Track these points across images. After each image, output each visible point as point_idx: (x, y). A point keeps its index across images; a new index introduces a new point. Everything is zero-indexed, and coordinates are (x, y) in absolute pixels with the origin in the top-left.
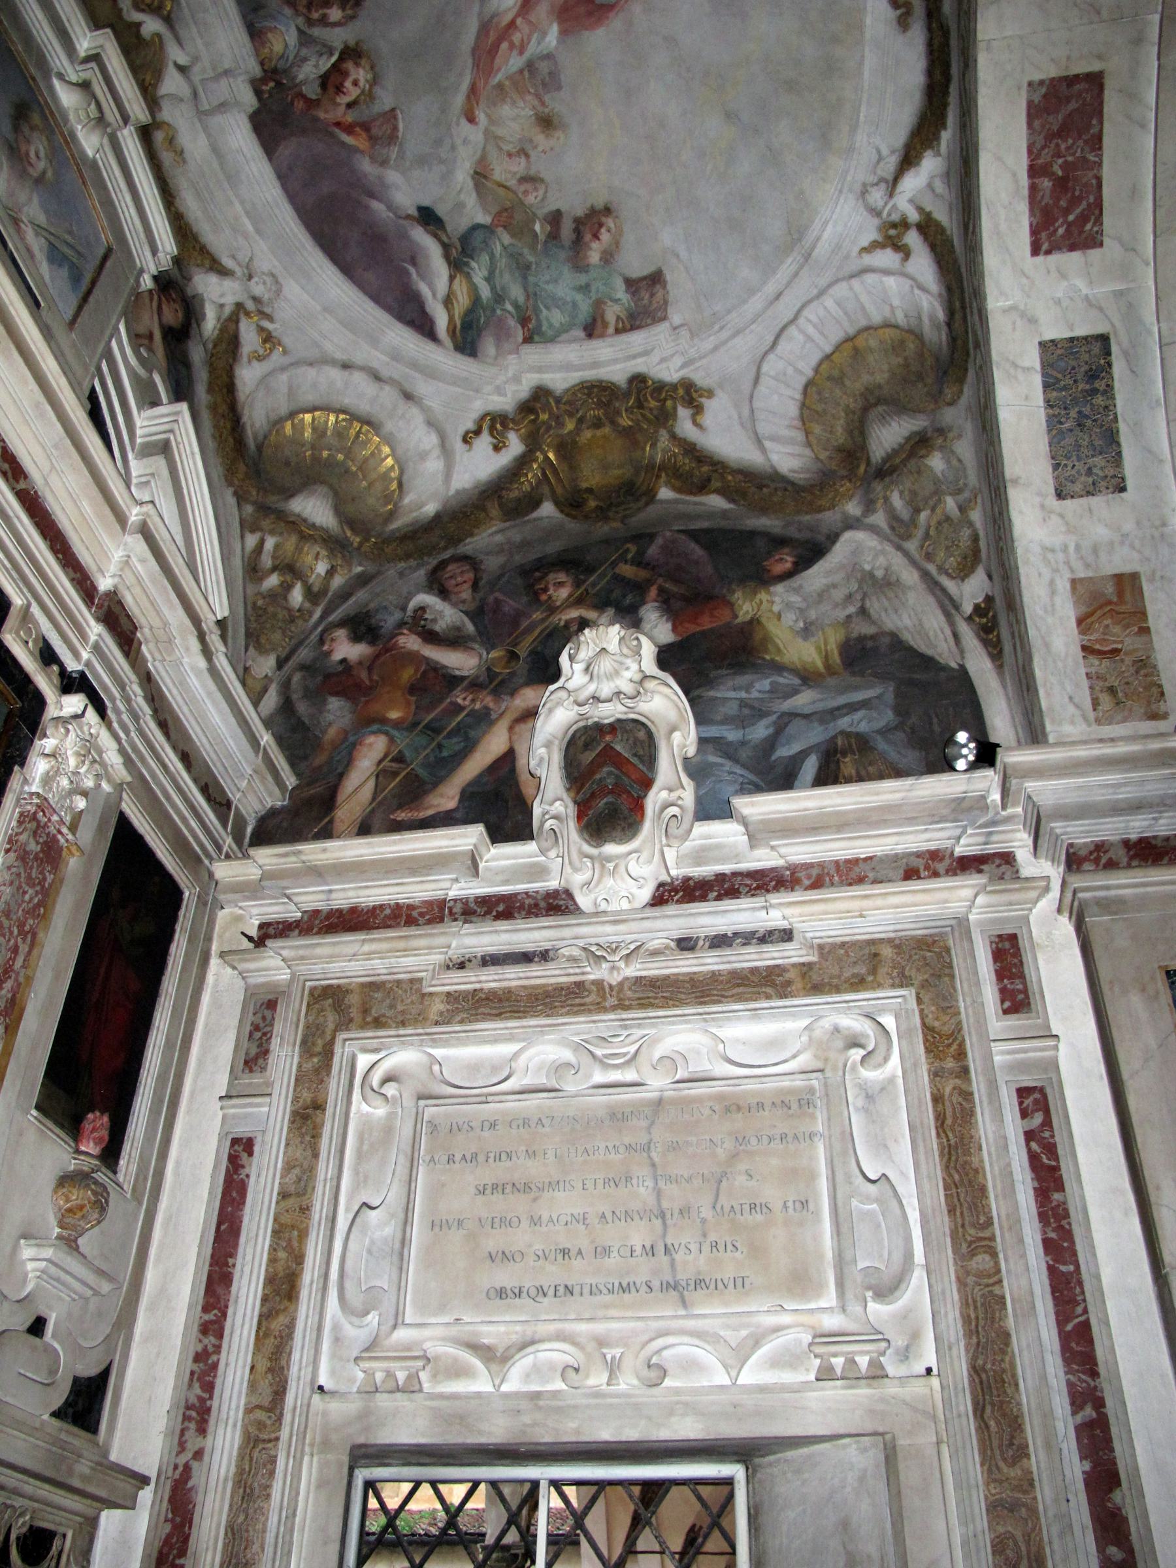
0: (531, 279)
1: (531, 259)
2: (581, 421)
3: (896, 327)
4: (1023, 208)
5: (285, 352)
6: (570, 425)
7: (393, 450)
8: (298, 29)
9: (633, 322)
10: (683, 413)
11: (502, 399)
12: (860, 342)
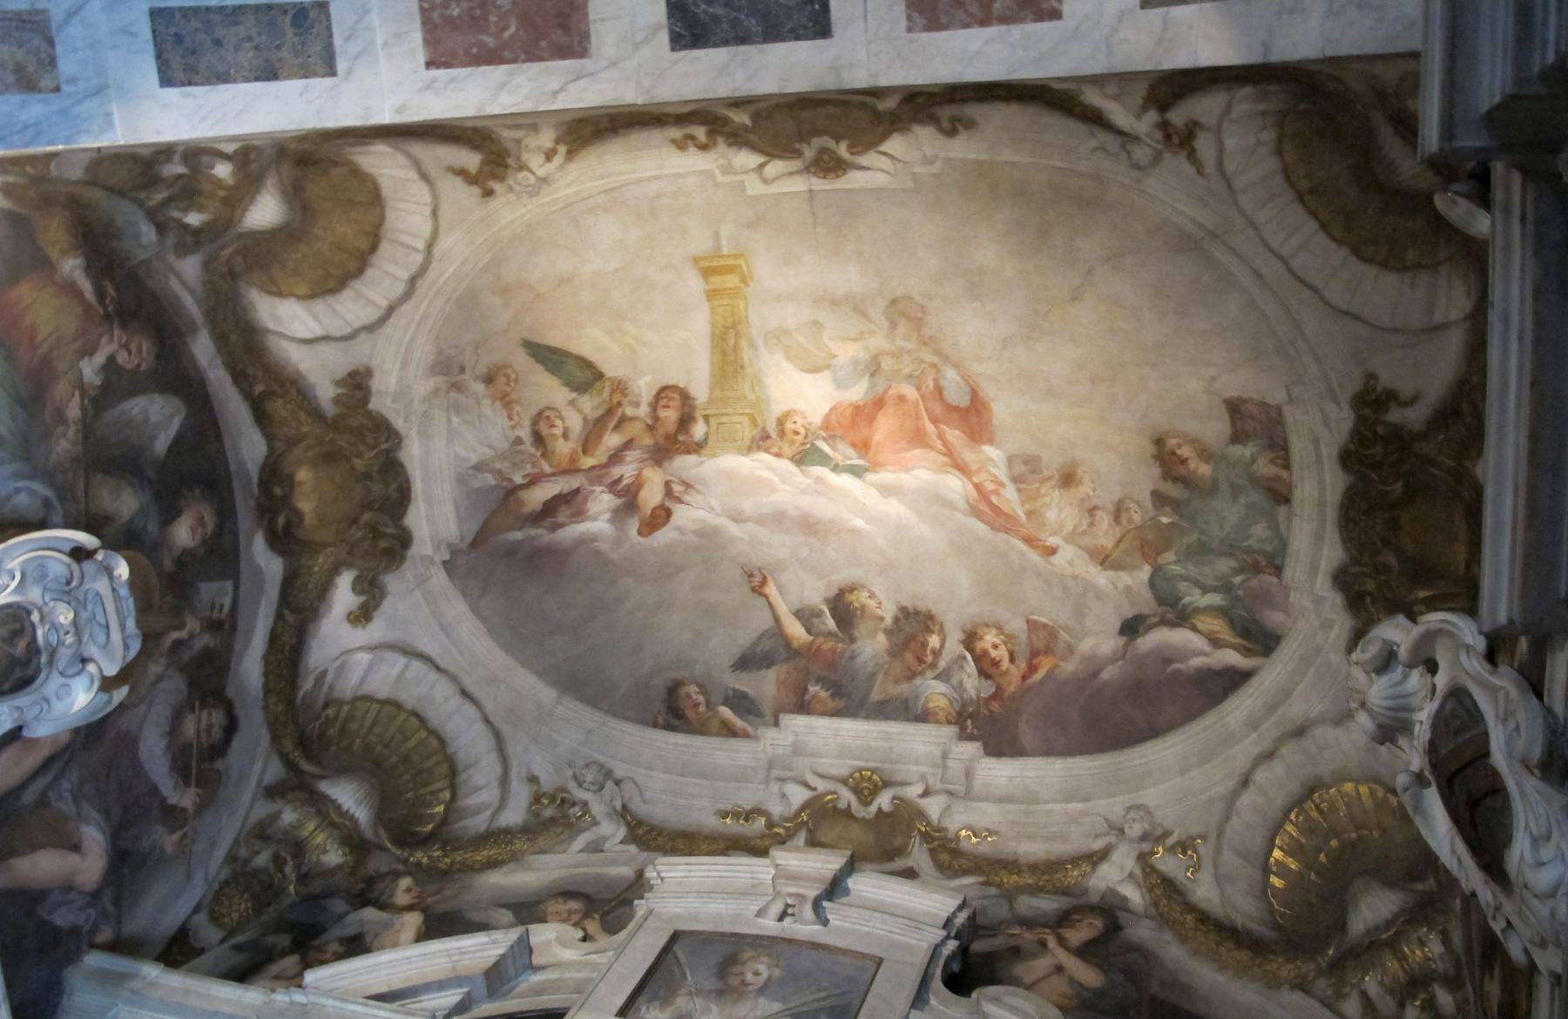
0: (1215, 544)
1: (1195, 537)
2: (1387, 544)
3: (1280, 140)
5: (1204, 838)
6: (1390, 558)
7: (1351, 780)
8: (937, 678)
9: (1278, 447)
10: (1395, 416)
11: (1336, 630)
12: (1304, 185)
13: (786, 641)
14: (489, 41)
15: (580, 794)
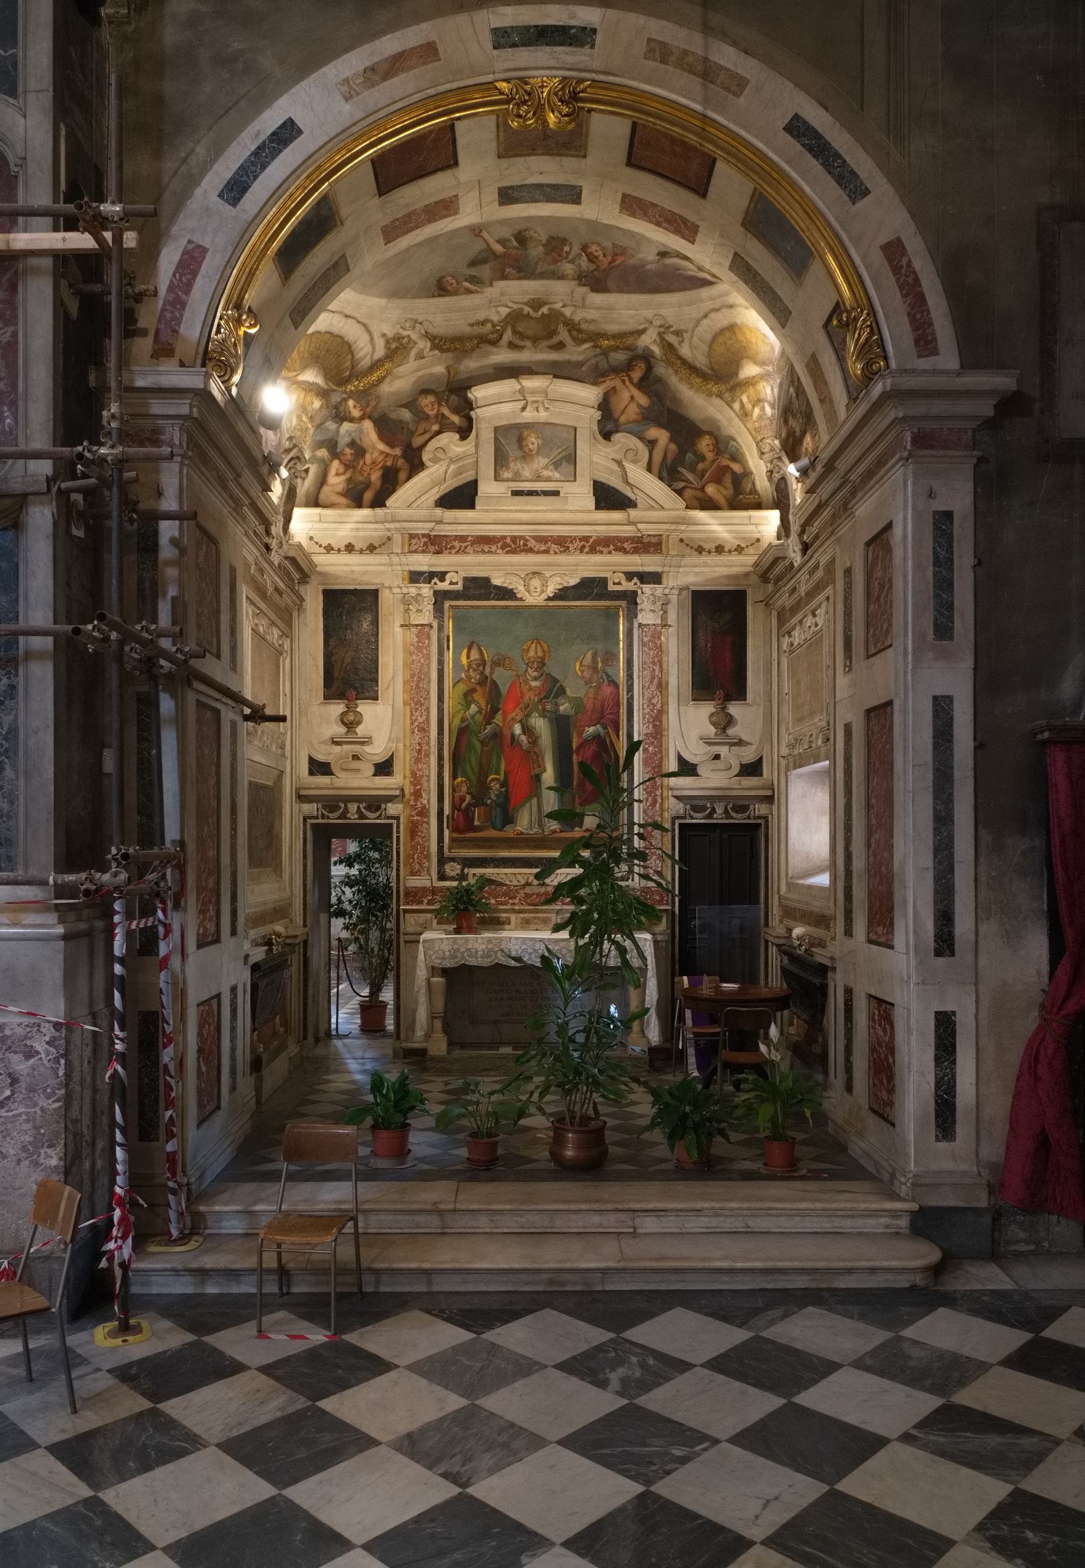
4: (672, 236)
13: (494, 253)
14: (412, 225)
15: (405, 333)
